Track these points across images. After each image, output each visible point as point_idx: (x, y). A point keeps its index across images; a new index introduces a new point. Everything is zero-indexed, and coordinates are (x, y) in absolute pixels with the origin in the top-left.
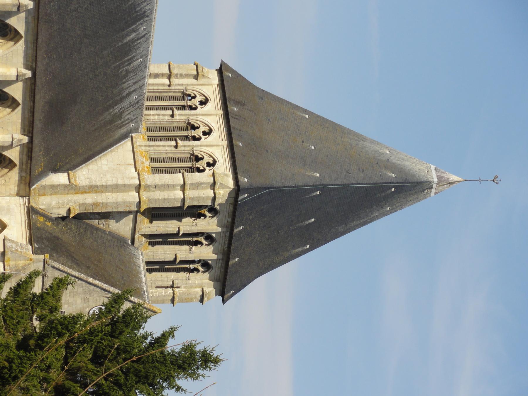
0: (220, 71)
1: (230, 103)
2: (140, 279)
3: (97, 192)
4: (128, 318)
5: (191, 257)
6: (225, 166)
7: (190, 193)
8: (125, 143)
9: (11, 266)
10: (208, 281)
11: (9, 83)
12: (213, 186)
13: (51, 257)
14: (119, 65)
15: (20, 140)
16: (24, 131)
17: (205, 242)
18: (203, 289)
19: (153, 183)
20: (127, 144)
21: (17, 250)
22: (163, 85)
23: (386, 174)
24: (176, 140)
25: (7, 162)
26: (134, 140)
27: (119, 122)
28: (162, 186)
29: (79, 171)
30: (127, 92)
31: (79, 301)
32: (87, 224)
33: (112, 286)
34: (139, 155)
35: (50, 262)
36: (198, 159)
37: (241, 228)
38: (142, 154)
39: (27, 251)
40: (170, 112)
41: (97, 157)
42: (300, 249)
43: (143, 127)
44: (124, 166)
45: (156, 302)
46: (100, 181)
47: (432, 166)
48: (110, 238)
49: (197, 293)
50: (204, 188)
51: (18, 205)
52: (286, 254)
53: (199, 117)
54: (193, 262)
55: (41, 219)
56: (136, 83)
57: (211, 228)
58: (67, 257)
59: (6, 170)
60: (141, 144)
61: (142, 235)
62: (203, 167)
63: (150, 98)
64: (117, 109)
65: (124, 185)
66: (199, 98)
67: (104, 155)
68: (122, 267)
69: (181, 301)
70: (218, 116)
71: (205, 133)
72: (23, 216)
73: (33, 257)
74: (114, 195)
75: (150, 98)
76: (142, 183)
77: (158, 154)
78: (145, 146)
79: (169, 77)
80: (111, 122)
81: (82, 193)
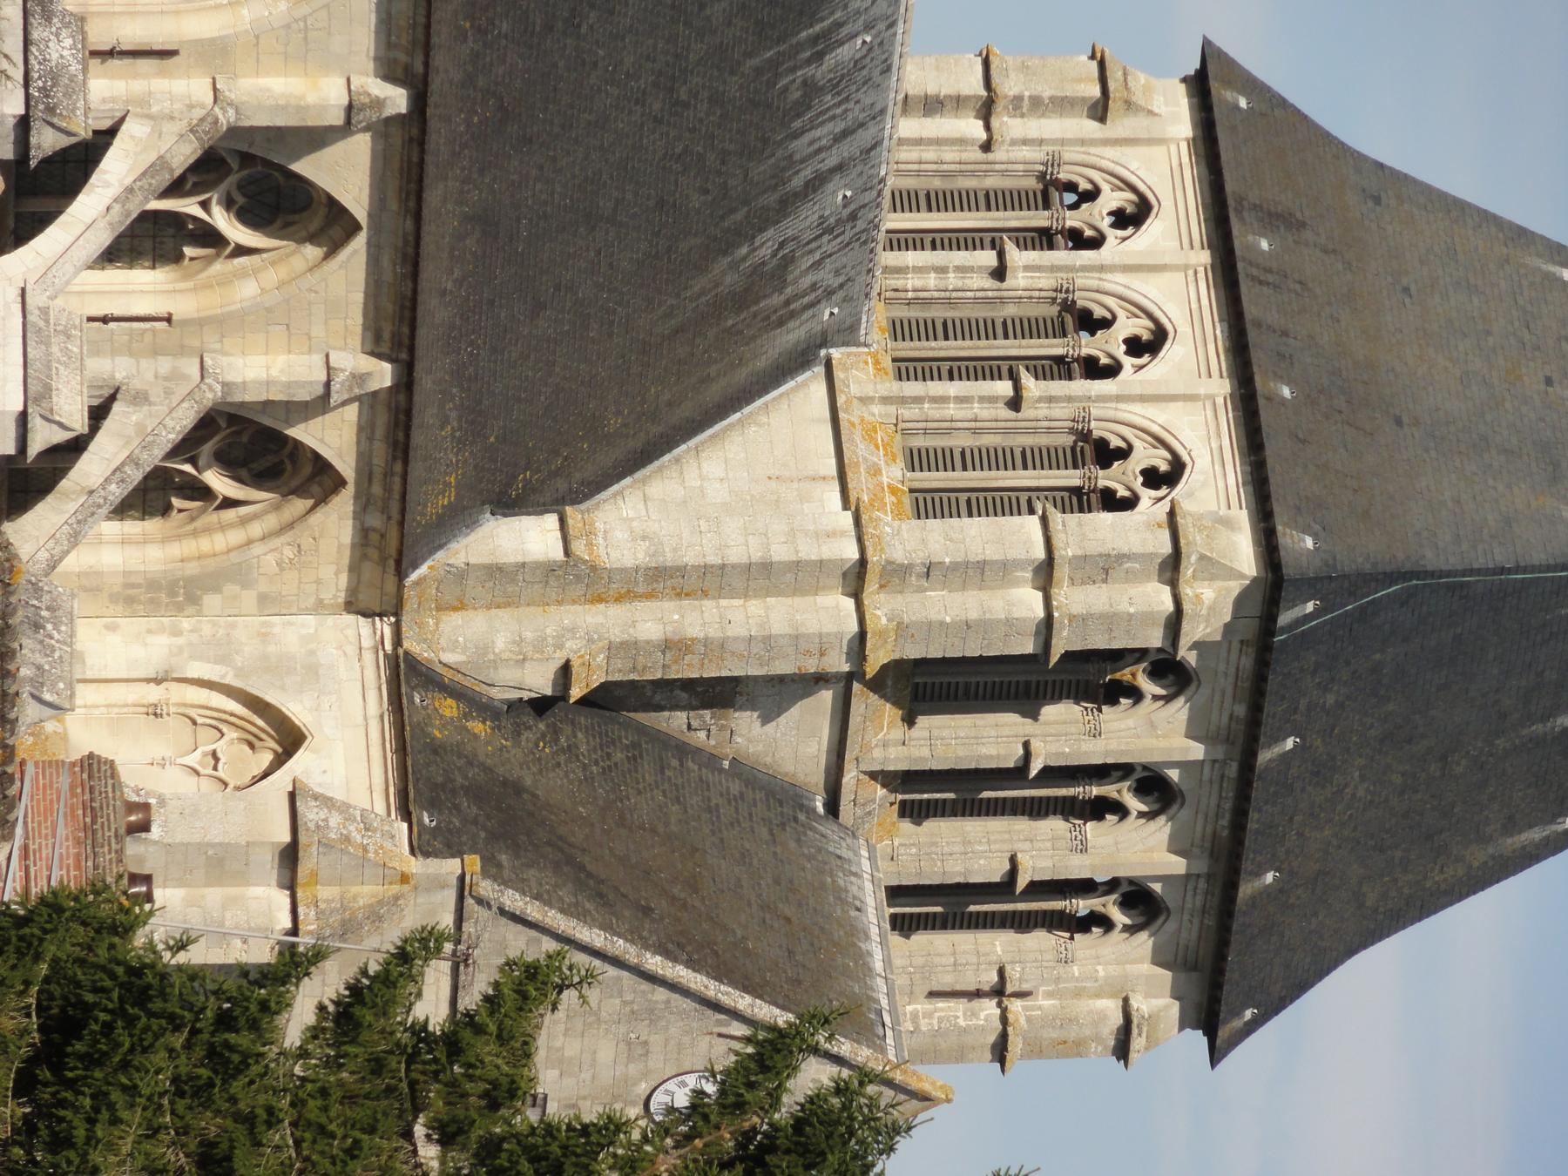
0: (1199, 85)
1: (1242, 219)
2: (862, 958)
3: (680, 594)
4: (816, 1133)
5: (1077, 867)
6: (1221, 484)
7: (1072, 598)
8: (798, 387)
9: (322, 906)
10: (1147, 968)
11: (315, 138)
12: (1171, 568)
13: (491, 868)
14: (774, 64)
15: (360, 378)
16: (378, 338)
17: (1134, 804)
19: (919, 558)
20: (808, 391)
21: (347, 839)
22: (961, 142)
24: (1014, 378)
25: (307, 470)
26: (839, 374)
27: (776, 300)
28: (955, 566)
29: (607, 507)
30: (807, 173)
31: (606, 1052)
32: (642, 730)
33: (747, 988)
34: (857, 437)
35: (486, 888)
36: (1107, 455)
37: (1290, 743)
38: (870, 432)
39: (388, 845)
40: (988, 258)
41: (683, 447)
42: (1536, 834)
43: (875, 320)
44: (795, 485)
45: (931, 1054)
46: (696, 550)
48: (735, 787)
49: (1102, 1016)
50: (1131, 577)
51: (352, 650)
52: (1478, 856)
53: (1109, 276)
54: (1086, 887)
55: (449, 708)
56: (846, 134)
57: (1163, 743)
58: (557, 867)
59: (300, 505)
60: (869, 390)
61: (873, 775)
62: (1129, 489)
63: (906, 201)
64: (766, 246)
65: (797, 566)
66: (1112, 199)
67: (712, 437)
68: (788, 910)
69: (1036, 1050)
70: (1191, 272)
71: (1136, 347)
72: (372, 696)
73: (416, 866)
74: (755, 607)
75: (906, 201)
76: (873, 558)
77: (937, 432)
78: (886, 400)
79: (986, 110)
80: (742, 299)
81: (619, 599)
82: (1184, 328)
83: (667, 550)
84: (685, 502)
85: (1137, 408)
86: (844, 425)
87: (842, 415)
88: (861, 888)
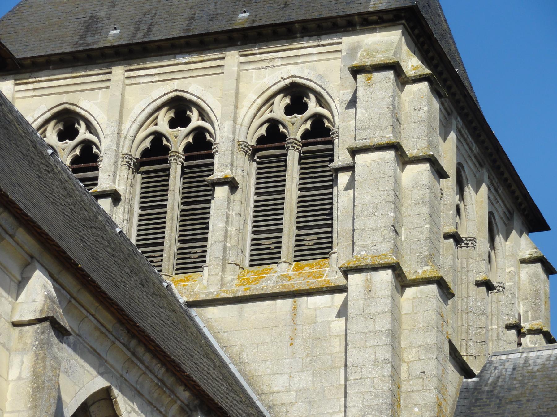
6: (315, 58)
8: (210, 328)
18: (524, 261)
26: (202, 297)
41: (258, 403)
44: (299, 327)
53: (124, 132)
62: (307, 120)
67: (250, 384)
70: (127, 81)
82: (176, 85)
83: (376, 402)
84: (310, 402)
85: (242, 112)
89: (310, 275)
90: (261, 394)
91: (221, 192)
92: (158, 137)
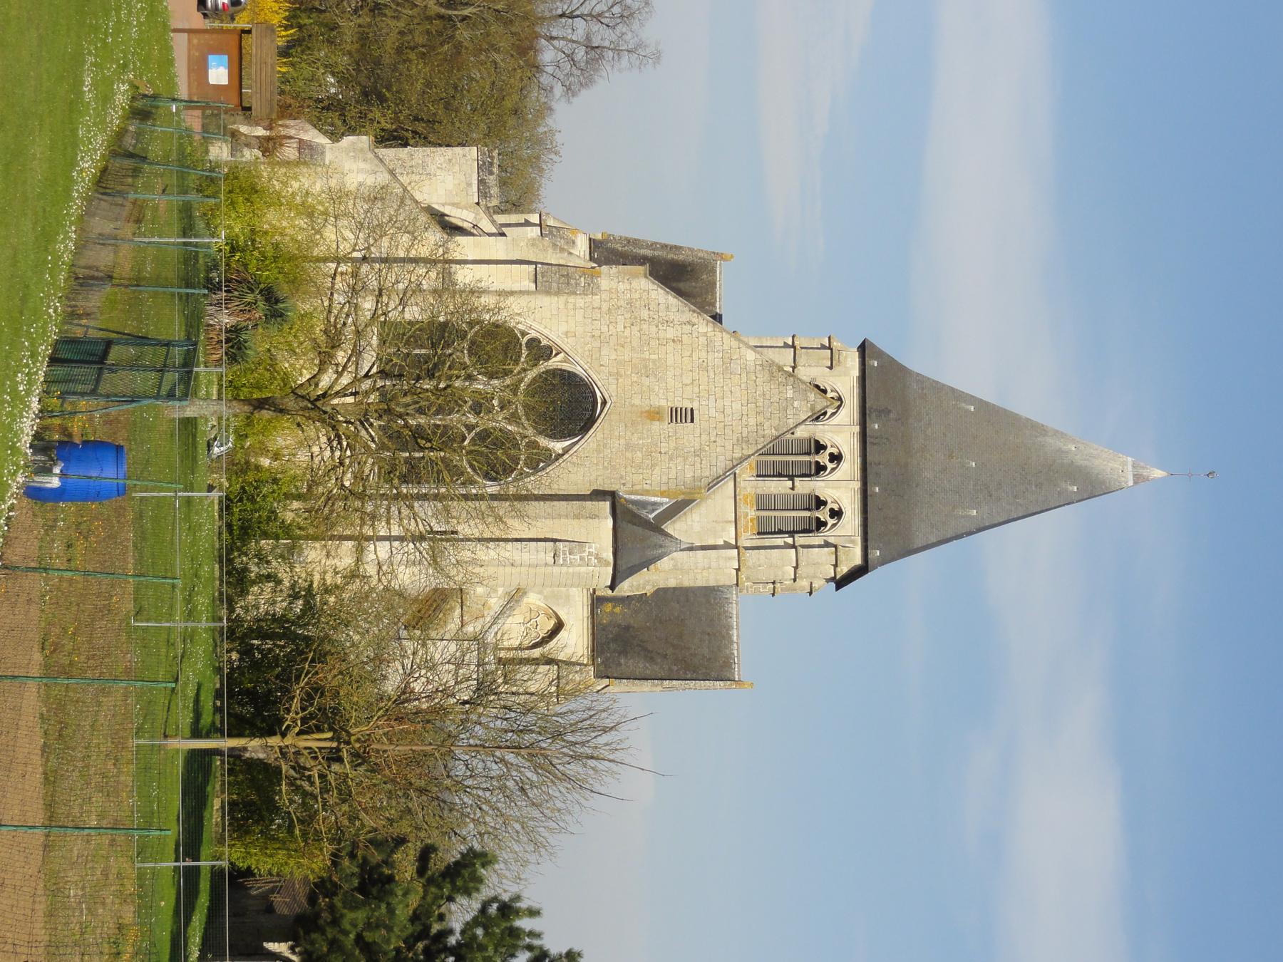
0: (863, 348)
23: (1066, 490)
26: (738, 480)
47: (1130, 459)
72: (585, 607)
86: (738, 501)
87: (738, 497)
88: (732, 608)
89: (746, 527)
90: (692, 509)
91: (790, 483)
92: (824, 448)
